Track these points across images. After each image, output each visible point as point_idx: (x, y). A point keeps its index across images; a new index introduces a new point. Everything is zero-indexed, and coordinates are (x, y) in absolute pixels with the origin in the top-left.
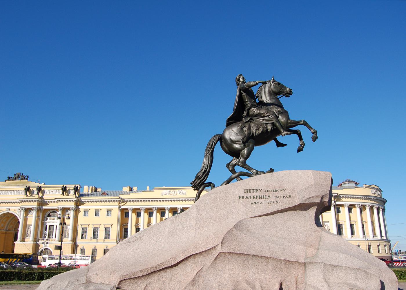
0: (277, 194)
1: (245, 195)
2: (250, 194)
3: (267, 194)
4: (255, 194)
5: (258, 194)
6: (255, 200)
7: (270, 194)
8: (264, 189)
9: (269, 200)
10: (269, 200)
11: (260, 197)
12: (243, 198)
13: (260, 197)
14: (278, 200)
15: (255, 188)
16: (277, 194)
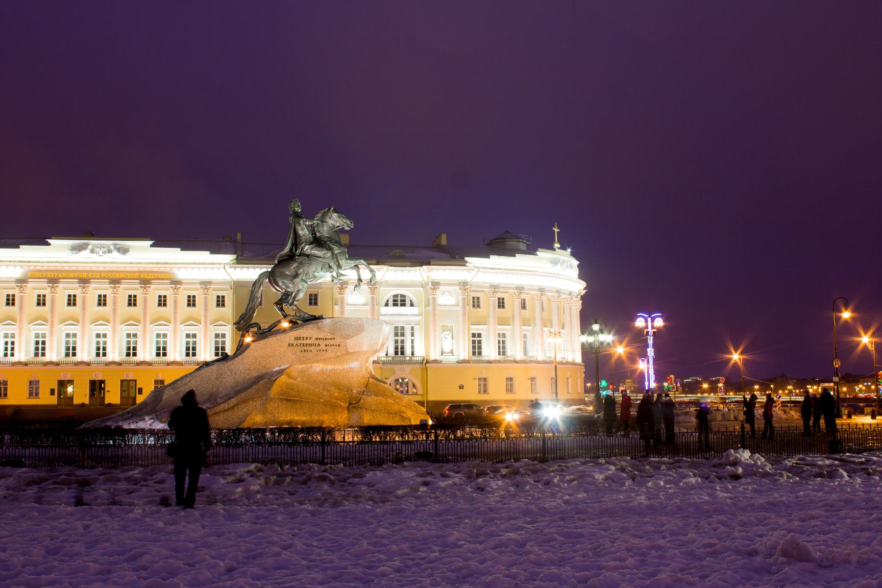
0: (327, 342)
1: (295, 343)
2: (299, 342)
3: (317, 342)
4: (305, 342)
5: (308, 342)
6: (305, 348)
7: (320, 342)
8: (314, 337)
9: (319, 348)
10: (319, 348)
11: (310, 345)
12: (292, 345)
13: (310, 345)
14: (327, 348)
15: (305, 336)
16: (327, 342)
